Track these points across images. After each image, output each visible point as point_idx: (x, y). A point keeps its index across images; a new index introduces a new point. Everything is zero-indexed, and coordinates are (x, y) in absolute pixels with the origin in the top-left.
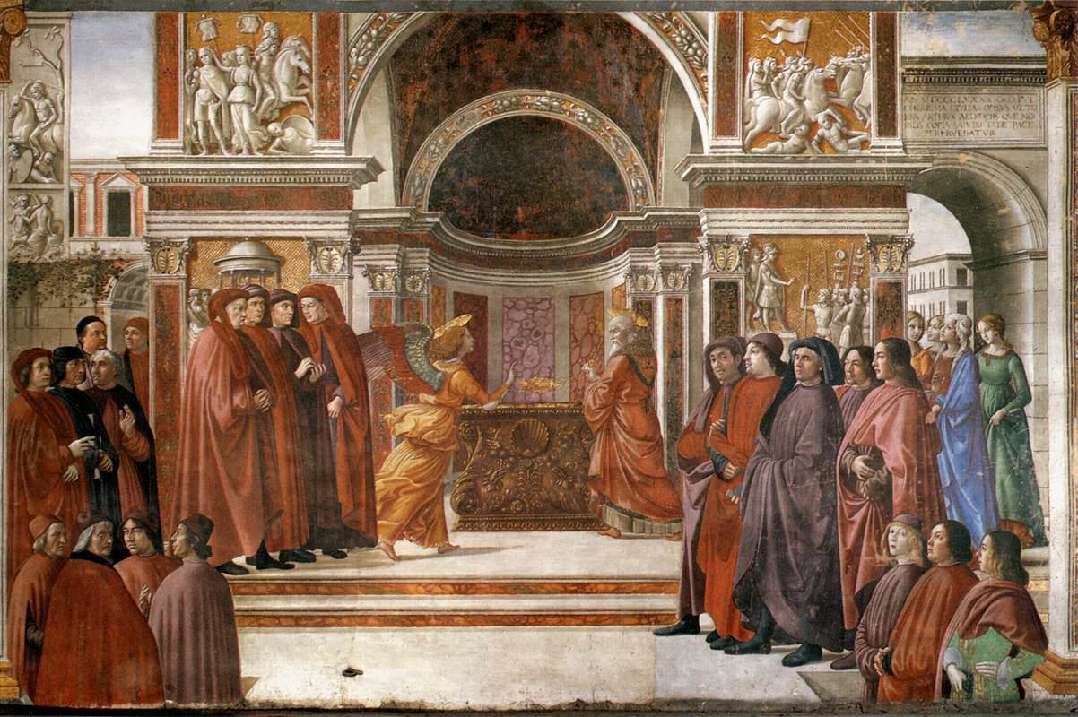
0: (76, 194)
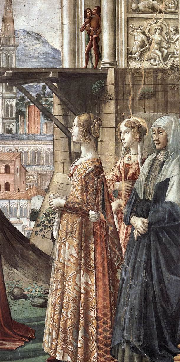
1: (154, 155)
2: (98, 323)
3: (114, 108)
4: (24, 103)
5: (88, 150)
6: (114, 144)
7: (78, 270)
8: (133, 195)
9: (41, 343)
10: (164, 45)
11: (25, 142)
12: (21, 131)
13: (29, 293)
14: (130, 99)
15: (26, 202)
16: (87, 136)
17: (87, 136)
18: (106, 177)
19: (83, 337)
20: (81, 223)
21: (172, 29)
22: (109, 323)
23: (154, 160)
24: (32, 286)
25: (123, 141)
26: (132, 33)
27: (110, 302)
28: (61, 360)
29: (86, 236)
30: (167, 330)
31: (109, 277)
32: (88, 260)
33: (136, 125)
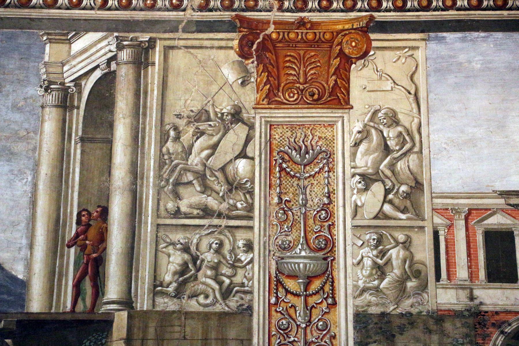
0: (441, 233)
10: (225, 270)
21: (241, 243)
26: (164, 249)
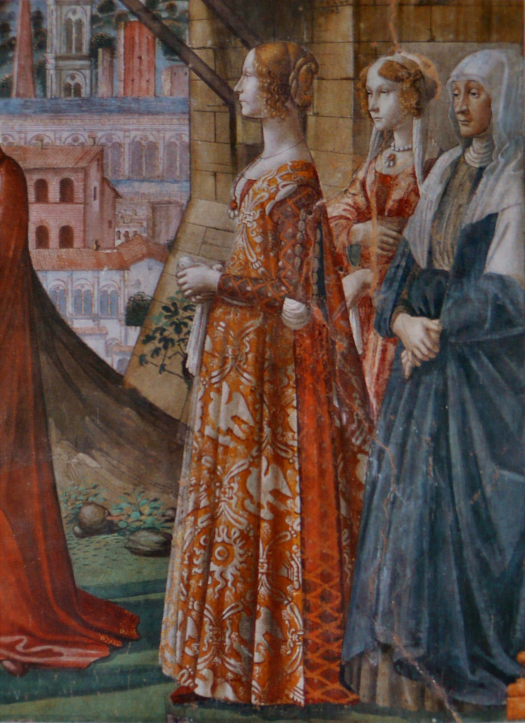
1: (455, 152)
2: (308, 597)
3: (351, 29)
4: (113, 15)
5: (280, 140)
6: (350, 123)
7: (254, 458)
8: (399, 258)
9: (155, 652)
11: (115, 117)
12: (103, 90)
13: (123, 518)
14: (392, 6)
15: (116, 276)
16: (278, 100)
17: (278, 100)
18: (329, 210)
19: (267, 636)
20: (260, 332)
22: (337, 597)
23: (456, 165)
24: (130, 499)
25: (373, 114)
27: (340, 543)
28: (209, 695)
29: (275, 368)
30: (490, 615)
31: (336, 476)
32: (280, 430)
33: (410, 74)
